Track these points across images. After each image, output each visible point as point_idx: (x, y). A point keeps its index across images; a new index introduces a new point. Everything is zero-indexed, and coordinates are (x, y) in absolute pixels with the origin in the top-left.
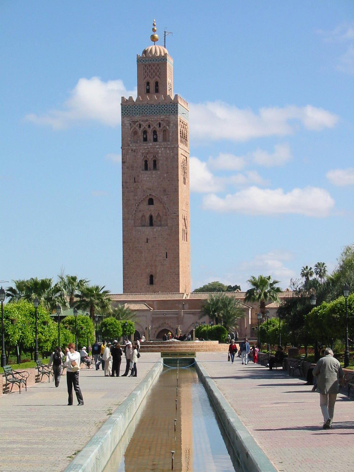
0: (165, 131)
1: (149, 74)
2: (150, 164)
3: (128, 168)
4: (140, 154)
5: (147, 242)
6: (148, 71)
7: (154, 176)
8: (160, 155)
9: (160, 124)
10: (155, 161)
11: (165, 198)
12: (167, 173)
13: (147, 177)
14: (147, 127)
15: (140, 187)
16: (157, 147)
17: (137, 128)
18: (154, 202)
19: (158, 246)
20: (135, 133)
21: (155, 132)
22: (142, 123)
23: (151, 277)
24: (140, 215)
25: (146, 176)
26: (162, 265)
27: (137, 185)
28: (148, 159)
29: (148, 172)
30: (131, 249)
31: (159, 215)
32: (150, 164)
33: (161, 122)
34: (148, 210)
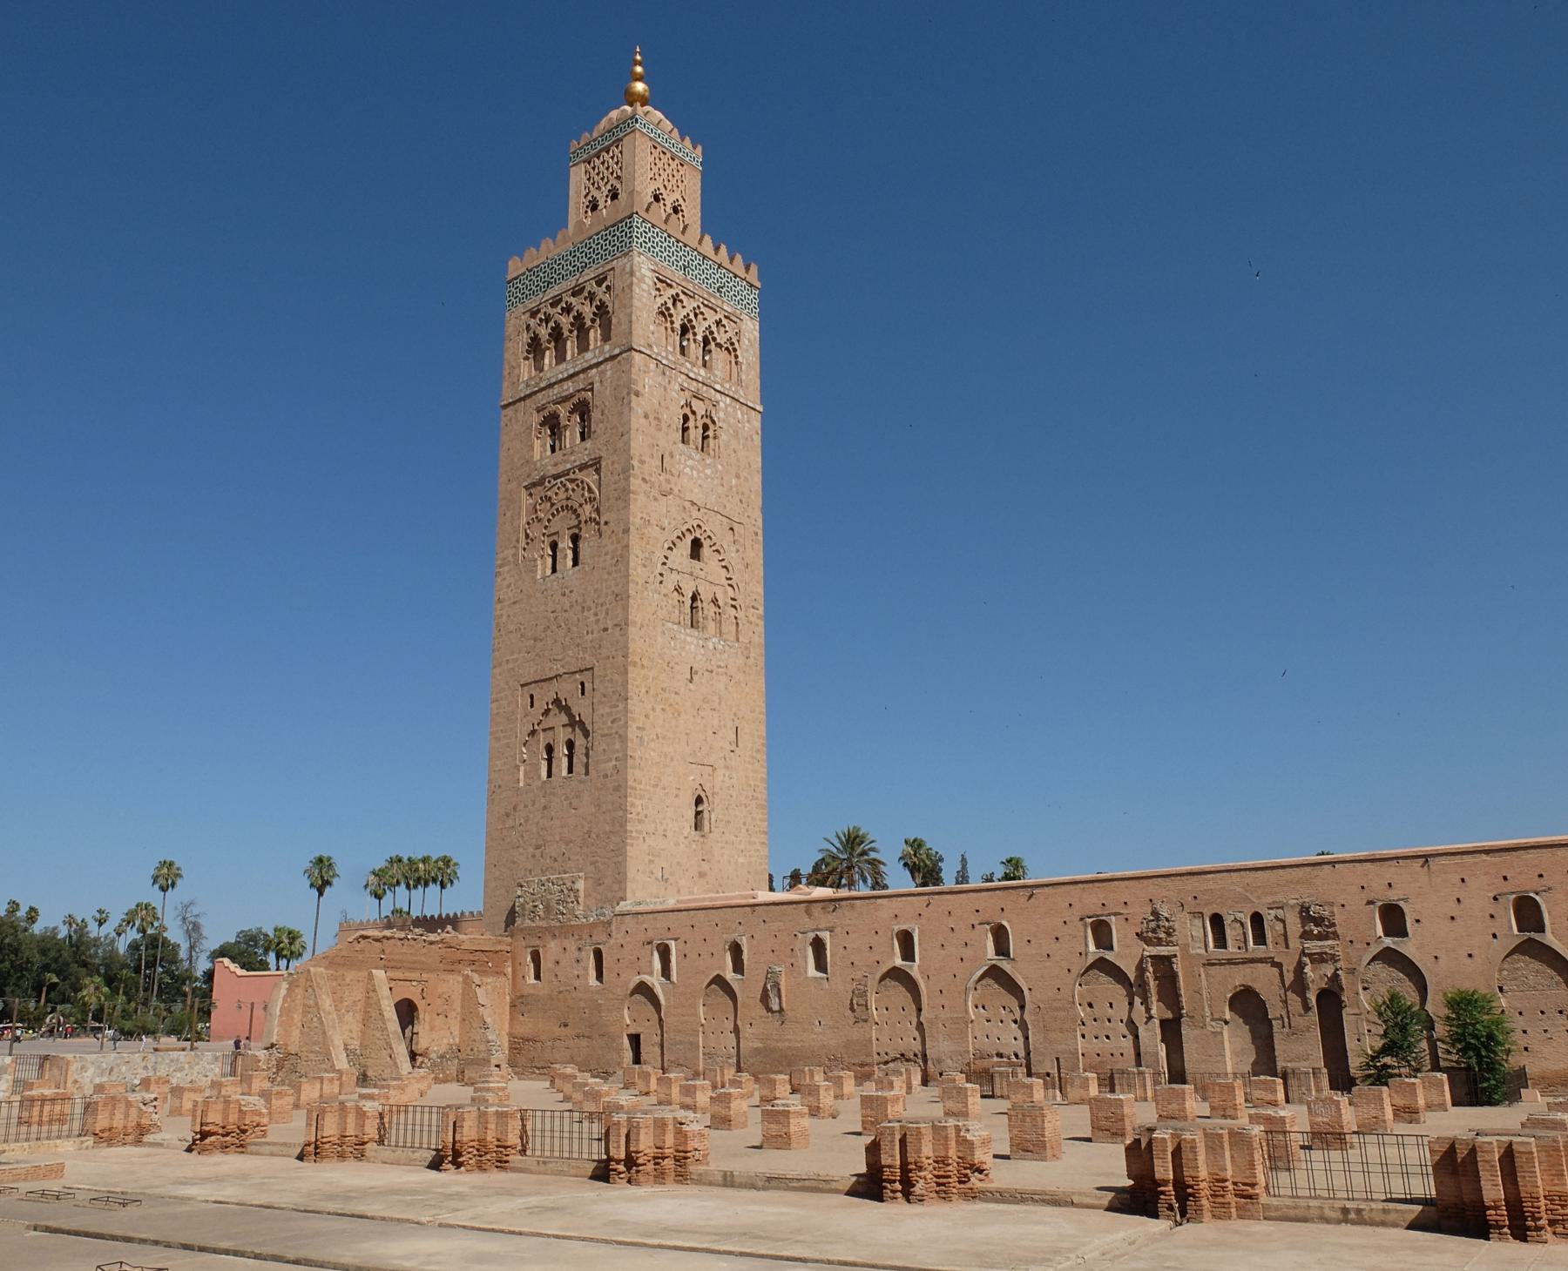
0: (731, 349)
1: (664, 176)
2: (695, 434)
3: (646, 417)
4: (677, 387)
5: (691, 681)
6: (660, 165)
7: (708, 472)
8: (721, 415)
9: (718, 323)
10: (705, 427)
11: (732, 556)
12: (738, 477)
13: (692, 468)
14: (692, 316)
15: (676, 491)
16: (718, 387)
17: (670, 305)
18: (706, 551)
19: (716, 698)
20: (664, 313)
21: (706, 341)
22: (682, 297)
23: (699, 801)
24: (671, 580)
25: (690, 462)
26: (727, 767)
27: (668, 481)
28: (694, 413)
29: (690, 450)
30: (652, 692)
31: (715, 601)
32: (695, 434)
33: (725, 322)
34: (691, 574)
